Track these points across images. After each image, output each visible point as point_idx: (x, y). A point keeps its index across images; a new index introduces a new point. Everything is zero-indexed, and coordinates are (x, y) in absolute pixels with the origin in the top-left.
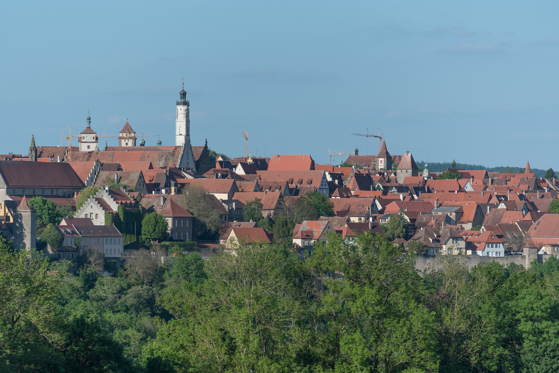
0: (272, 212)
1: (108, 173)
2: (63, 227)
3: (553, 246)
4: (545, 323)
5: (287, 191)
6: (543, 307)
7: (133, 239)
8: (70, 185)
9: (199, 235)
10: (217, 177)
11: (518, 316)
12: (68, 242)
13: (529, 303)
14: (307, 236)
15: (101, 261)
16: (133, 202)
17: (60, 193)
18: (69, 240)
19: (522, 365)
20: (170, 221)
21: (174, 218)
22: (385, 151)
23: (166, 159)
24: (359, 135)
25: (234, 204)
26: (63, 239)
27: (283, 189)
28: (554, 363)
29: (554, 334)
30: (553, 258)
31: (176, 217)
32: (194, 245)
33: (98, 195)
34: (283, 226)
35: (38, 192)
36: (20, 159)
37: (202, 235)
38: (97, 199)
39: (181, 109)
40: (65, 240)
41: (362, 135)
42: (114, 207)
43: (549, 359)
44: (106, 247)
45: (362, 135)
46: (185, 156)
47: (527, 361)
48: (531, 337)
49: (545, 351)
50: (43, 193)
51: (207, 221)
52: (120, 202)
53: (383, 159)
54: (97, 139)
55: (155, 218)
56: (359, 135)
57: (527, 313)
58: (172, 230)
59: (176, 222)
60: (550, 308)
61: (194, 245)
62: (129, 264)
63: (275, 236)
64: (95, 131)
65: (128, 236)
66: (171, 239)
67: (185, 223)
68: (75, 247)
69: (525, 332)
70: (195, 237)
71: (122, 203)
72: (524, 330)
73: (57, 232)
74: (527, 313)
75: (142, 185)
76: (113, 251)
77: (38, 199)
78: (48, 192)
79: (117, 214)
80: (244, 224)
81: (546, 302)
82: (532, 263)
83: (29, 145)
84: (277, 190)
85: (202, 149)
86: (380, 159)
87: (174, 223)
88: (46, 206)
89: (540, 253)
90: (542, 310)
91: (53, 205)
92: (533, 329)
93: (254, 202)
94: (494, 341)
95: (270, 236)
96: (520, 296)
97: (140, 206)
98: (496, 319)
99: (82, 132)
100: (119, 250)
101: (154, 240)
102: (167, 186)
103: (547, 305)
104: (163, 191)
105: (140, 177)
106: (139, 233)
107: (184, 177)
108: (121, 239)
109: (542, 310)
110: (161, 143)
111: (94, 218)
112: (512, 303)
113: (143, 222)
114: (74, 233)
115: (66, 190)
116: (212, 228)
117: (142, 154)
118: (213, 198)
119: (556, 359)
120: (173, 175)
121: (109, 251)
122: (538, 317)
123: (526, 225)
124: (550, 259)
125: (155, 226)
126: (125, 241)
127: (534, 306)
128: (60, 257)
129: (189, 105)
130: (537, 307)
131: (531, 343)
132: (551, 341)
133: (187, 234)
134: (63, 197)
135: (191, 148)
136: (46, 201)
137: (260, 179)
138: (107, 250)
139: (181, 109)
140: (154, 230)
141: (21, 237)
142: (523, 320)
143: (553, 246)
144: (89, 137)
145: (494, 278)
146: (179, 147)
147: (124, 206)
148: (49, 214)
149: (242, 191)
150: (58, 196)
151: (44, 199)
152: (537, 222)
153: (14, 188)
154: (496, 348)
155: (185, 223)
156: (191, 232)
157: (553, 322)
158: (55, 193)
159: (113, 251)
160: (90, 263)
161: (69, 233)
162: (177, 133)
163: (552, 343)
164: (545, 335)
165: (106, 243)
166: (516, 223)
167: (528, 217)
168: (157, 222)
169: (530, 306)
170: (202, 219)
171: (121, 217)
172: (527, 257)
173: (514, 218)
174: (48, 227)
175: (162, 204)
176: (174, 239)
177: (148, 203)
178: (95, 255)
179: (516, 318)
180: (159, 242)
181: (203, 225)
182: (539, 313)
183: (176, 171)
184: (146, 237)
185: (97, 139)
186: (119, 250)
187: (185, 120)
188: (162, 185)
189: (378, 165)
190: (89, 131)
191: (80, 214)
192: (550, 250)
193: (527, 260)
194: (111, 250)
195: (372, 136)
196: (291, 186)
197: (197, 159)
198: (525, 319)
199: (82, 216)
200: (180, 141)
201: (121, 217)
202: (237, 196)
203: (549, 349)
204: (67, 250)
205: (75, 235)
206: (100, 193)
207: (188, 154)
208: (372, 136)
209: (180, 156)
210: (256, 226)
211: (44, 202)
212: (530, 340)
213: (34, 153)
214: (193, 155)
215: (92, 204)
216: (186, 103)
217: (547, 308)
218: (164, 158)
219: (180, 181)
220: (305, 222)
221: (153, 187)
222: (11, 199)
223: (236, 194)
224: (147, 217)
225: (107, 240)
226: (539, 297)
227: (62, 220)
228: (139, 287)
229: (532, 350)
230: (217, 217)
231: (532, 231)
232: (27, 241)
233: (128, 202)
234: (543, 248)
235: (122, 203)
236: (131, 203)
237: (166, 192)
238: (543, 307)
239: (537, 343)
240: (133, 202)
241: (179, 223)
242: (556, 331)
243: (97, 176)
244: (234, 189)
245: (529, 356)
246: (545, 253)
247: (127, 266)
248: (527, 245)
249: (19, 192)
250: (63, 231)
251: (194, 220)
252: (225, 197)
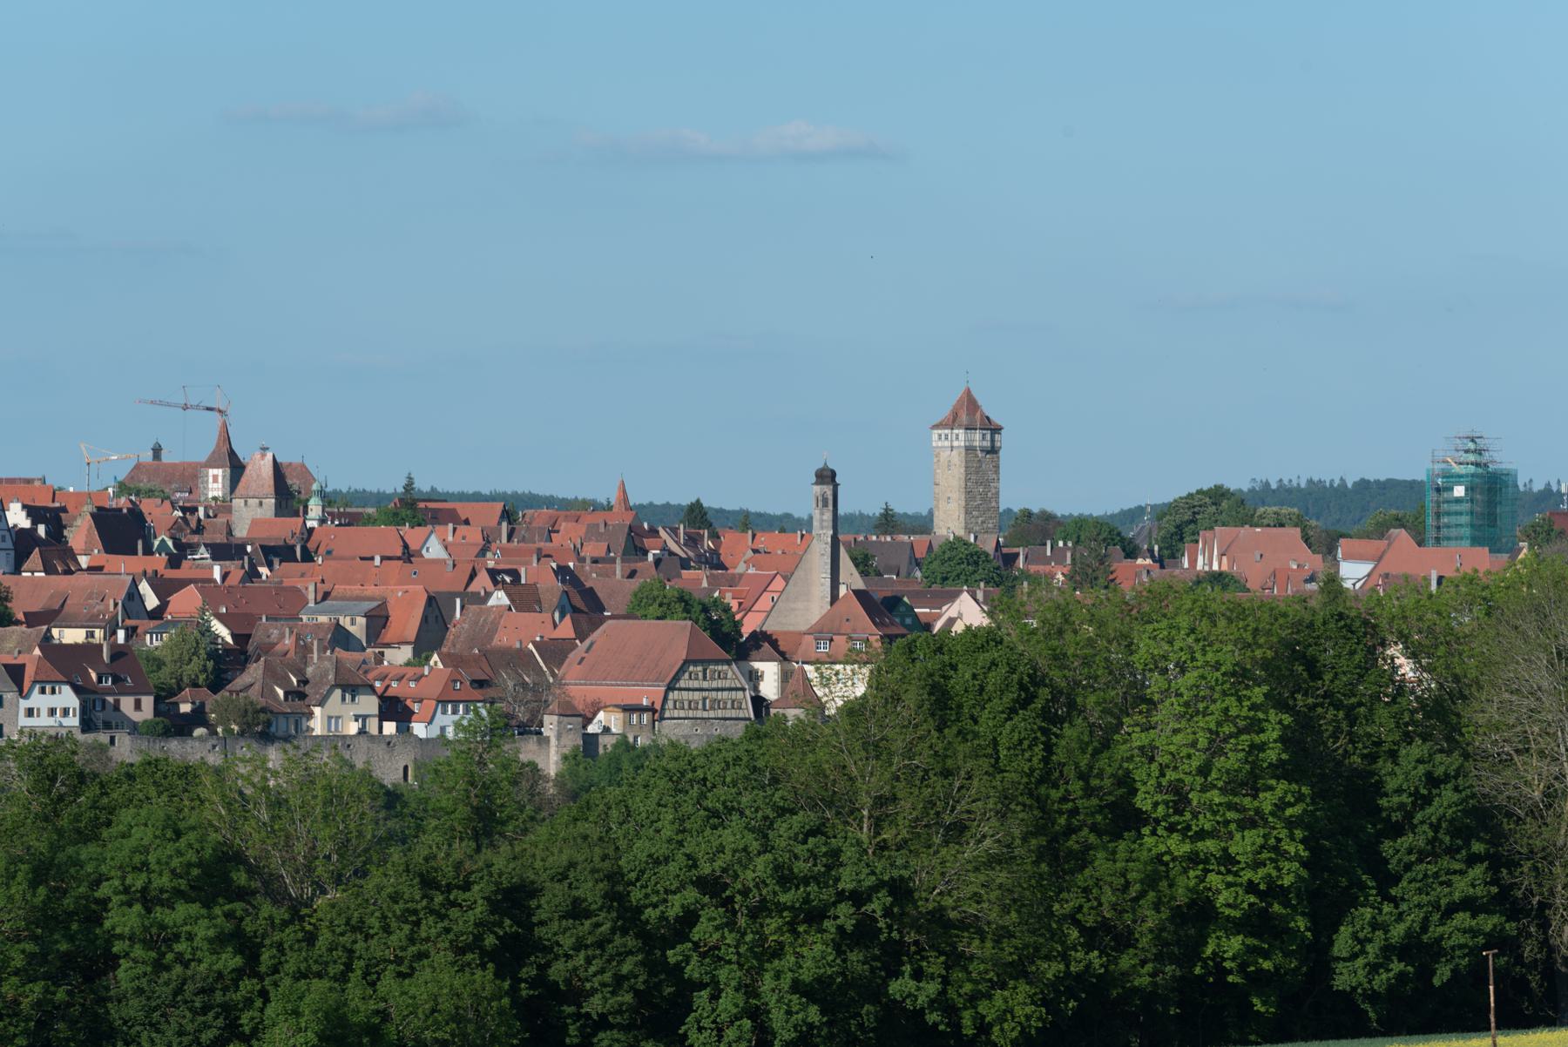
3: (628, 709)
4: (182, 910)
6: (175, 863)
11: (104, 890)
13: (135, 851)
19: (112, 1034)
22: (225, 449)
24: (161, 403)
28: (206, 1026)
29: (210, 941)
30: (624, 745)
41: (169, 405)
43: (188, 1015)
45: (169, 405)
47: (125, 1022)
48: (138, 952)
49: (179, 991)
53: (219, 472)
56: (161, 403)
57: (128, 882)
60: (200, 865)
69: (121, 937)
72: (118, 931)
74: (128, 882)
81: (190, 846)
82: (565, 758)
86: (212, 472)
89: (591, 729)
90: (173, 871)
92: (146, 929)
94: (18, 961)
96: (114, 830)
98: (28, 897)
103: (191, 856)
109: (173, 871)
112: (88, 851)
119: (211, 1014)
122: (162, 891)
123: (556, 652)
124: (615, 746)
127: (152, 859)
130: (159, 862)
131: (140, 969)
132: (200, 961)
142: (116, 899)
143: (628, 709)
145: (53, 780)
152: (587, 642)
154: (23, 985)
157: (207, 905)
163: (203, 967)
164: (181, 947)
166: (531, 646)
167: (566, 629)
169: (137, 859)
172: (553, 741)
173: (524, 632)
179: (99, 894)
182: (165, 881)
189: (206, 488)
192: (620, 722)
193: (553, 750)
195: (197, 407)
198: (123, 898)
203: (189, 988)
208: (197, 407)
212: (135, 961)
217: (190, 865)
226: (169, 834)
229: (139, 991)
231: (570, 669)
234: (601, 715)
238: (175, 863)
239: (159, 966)
242: (211, 933)
245: (133, 1008)
246: (607, 730)
248: (554, 707)
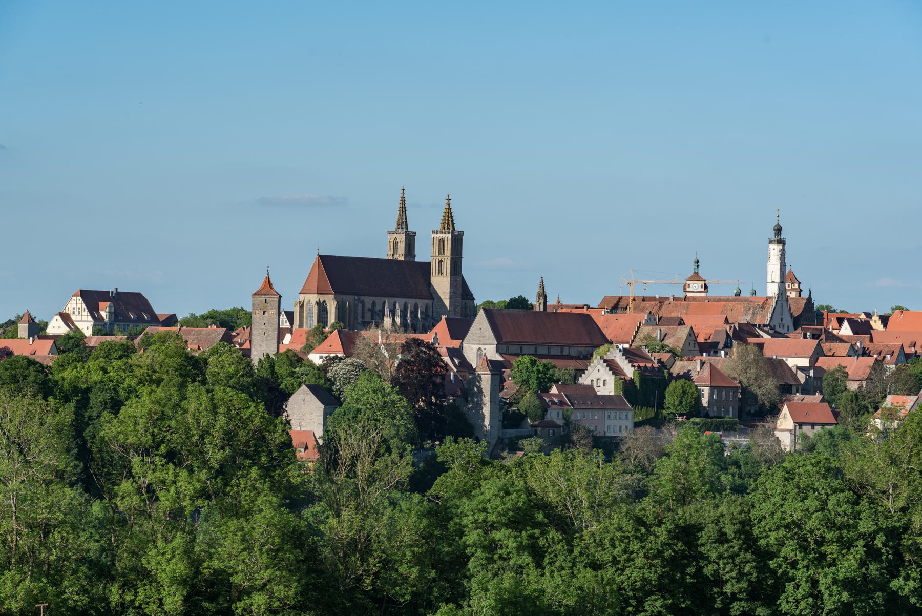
0: (864, 383)
1: (650, 328)
2: (555, 395)
5: (902, 358)
7: (652, 414)
8: (588, 342)
9: (753, 411)
10: (805, 337)
12: (555, 416)
14: (891, 414)
15: (590, 440)
16: (656, 365)
17: (574, 352)
18: (555, 413)
20: (706, 391)
21: (712, 388)
23: (753, 313)
25: (812, 371)
26: (546, 411)
27: (896, 354)
31: (715, 387)
32: (735, 424)
33: (609, 356)
34: (852, 402)
35: (526, 349)
36: (564, 310)
37: (753, 412)
38: (605, 361)
39: (775, 249)
40: (549, 411)
42: (629, 371)
44: (607, 423)
46: (778, 309)
50: (536, 351)
51: (759, 392)
52: (636, 365)
54: (706, 287)
55: (682, 387)
58: (709, 402)
59: (715, 392)
61: (735, 424)
62: (627, 446)
63: (843, 414)
64: (704, 278)
65: (644, 409)
66: (707, 416)
67: (727, 395)
68: (560, 422)
70: (740, 413)
71: (639, 367)
73: (538, 402)
75: (692, 343)
76: (624, 428)
77: (526, 359)
78: (542, 350)
79: (632, 381)
80: (808, 398)
83: (537, 289)
84: (876, 356)
85: (805, 301)
87: (711, 394)
88: (535, 369)
91: (545, 366)
93: (837, 370)
95: (836, 414)
97: (666, 371)
99: (687, 277)
100: (626, 427)
101: (681, 415)
102: (728, 346)
104: (723, 352)
105: (690, 335)
106: (661, 406)
107: (758, 336)
108: (631, 413)
110: (755, 293)
111: (602, 384)
113: (667, 392)
114: (562, 403)
115: (582, 349)
116: (766, 402)
117: (725, 306)
118: (781, 364)
120: (743, 333)
121: (612, 429)
125: (682, 398)
126: (635, 416)
128: (536, 434)
129: (784, 244)
133: (731, 409)
134: (577, 358)
135: (787, 300)
136: (535, 361)
137: (871, 340)
138: (609, 427)
139: (775, 249)
140: (681, 402)
141: (479, 405)
144: (696, 286)
146: (770, 298)
147: (642, 372)
148: (538, 378)
149: (833, 355)
150: (570, 357)
151: (534, 358)
153: (509, 344)
155: (727, 395)
156: (736, 407)
158: (566, 352)
159: (624, 428)
160: (573, 442)
161: (556, 404)
162: (769, 280)
165: (609, 417)
168: (684, 393)
170: (754, 390)
171: (637, 384)
174: (528, 395)
175: (699, 369)
176: (711, 415)
177: (683, 367)
178: (582, 433)
180: (688, 419)
181: (755, 396)
183: (747, 329)
184: (669, 411)
185: (706, 287)
186: (626, 427)
187: (779, 263)
188: (721, 346)
190: (696, 277)
191: (584, 380)
194: (621, 427)
196: (907, 350)
197: (796, 314)
199: (587, 382)
200: (772, 290)
201: (637, 384)
202: (822, 362)
204: (553, 425)
205: (566, 407)
206: (612, 353)
207: (782, 307)
209: (771, 310)
210: (822, 401)
211: (533, 363)
213: (542, 301)
214: (790, 309)
215: (599, 367)
216: (781, 242)
218: (751, 311)
219: (752, 340)
220: (889, 398)
221: (710, 347)
222: (499, 358)
223: (821, 359)
224: (673, 384)
225: (621, 414)
227: (550, 388)
228: (628, 476)
230: (773, 388)
232: (486, 410)
233: (649, 365)
235: (639, 367)
236: (653, 367)
237: (726, 354)
240: (656, 365)
241: (719, 395)
243: (637, 332)
244: (819, 353)
247: (624, 449)
249: (515, 349)
250: (547, 400)
251: (744, 390)
252: (805, 362)
